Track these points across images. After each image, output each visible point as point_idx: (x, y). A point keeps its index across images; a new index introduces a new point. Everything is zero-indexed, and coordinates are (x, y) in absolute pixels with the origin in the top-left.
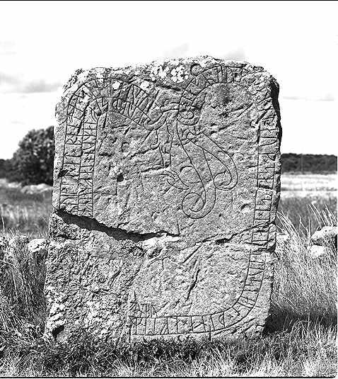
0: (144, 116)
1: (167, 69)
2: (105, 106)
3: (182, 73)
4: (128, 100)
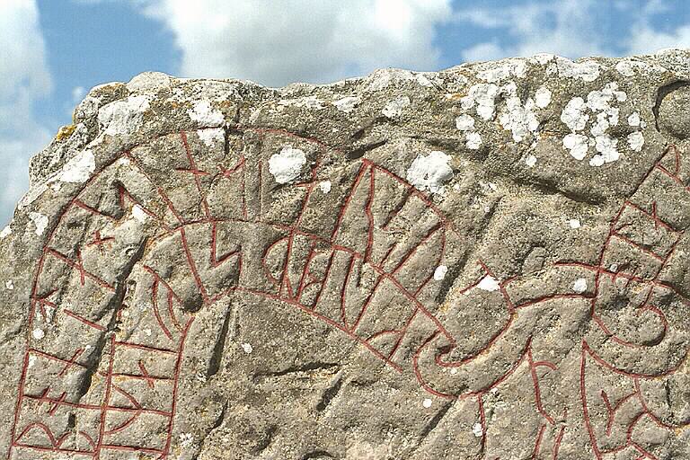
0: (422, 323)
1: (543, 98)
2: (226, 265)
3: (614, 121)
4: (344, 238)
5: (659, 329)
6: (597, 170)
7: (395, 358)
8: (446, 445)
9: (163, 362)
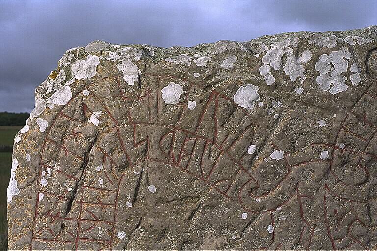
1: (306, 57)
5: (365, 177)
6: (335, 96)
7: (228, 194)
8: (253, 236)
9: (109, 197)
